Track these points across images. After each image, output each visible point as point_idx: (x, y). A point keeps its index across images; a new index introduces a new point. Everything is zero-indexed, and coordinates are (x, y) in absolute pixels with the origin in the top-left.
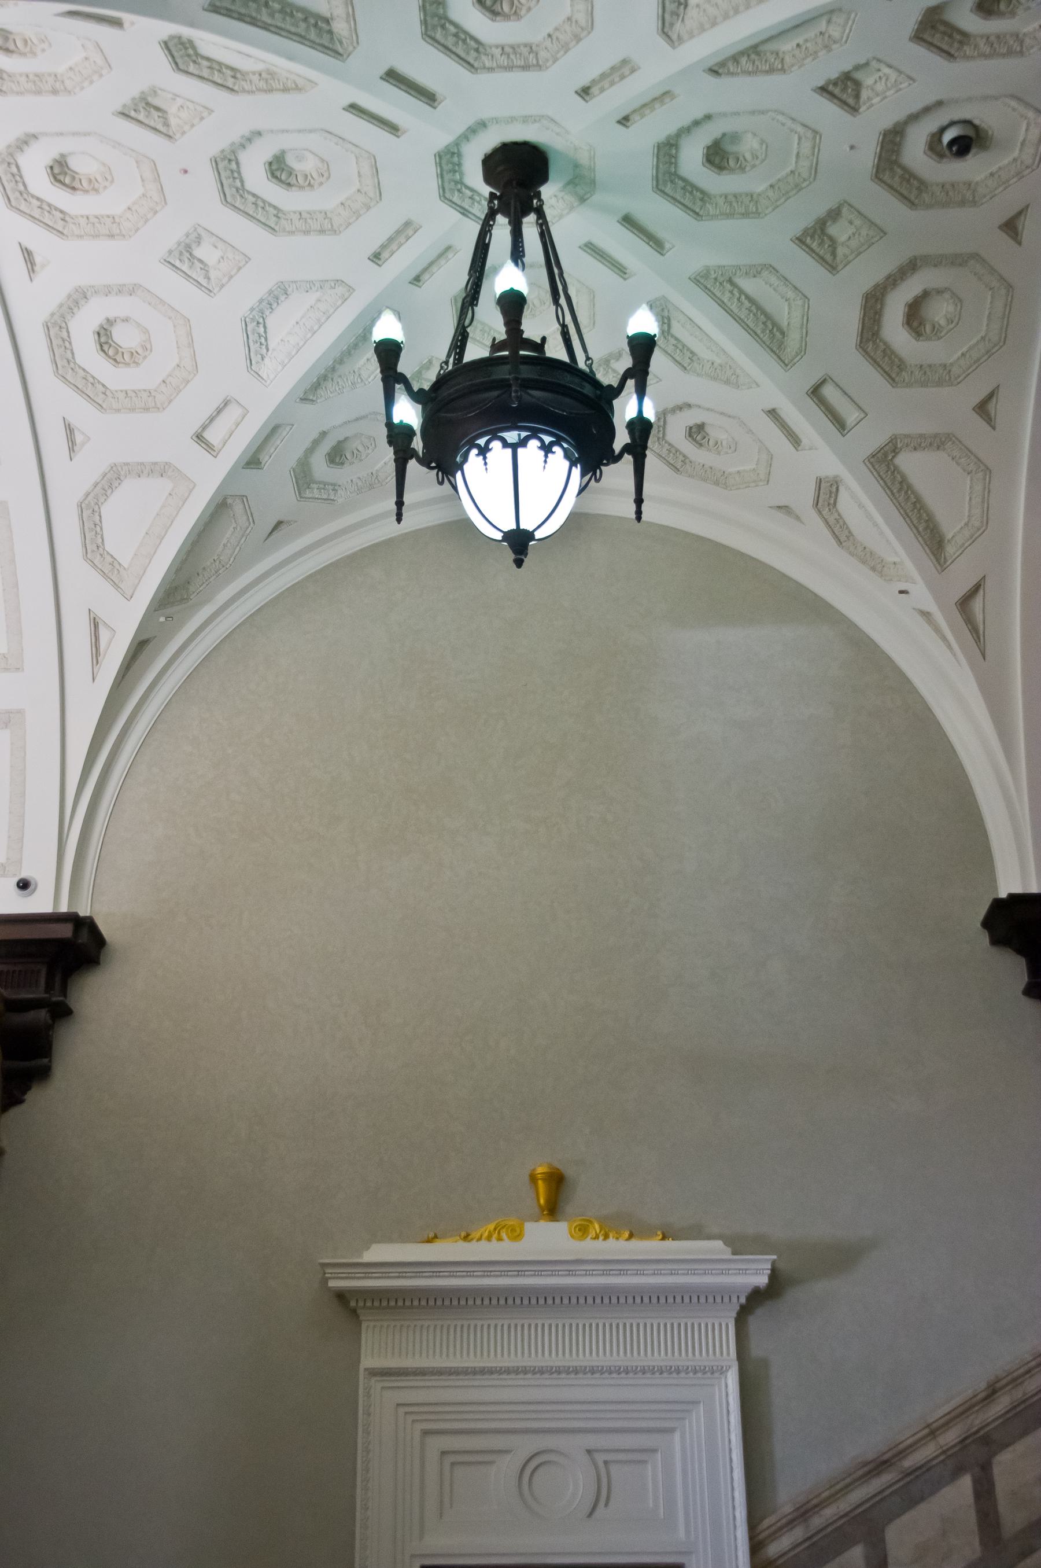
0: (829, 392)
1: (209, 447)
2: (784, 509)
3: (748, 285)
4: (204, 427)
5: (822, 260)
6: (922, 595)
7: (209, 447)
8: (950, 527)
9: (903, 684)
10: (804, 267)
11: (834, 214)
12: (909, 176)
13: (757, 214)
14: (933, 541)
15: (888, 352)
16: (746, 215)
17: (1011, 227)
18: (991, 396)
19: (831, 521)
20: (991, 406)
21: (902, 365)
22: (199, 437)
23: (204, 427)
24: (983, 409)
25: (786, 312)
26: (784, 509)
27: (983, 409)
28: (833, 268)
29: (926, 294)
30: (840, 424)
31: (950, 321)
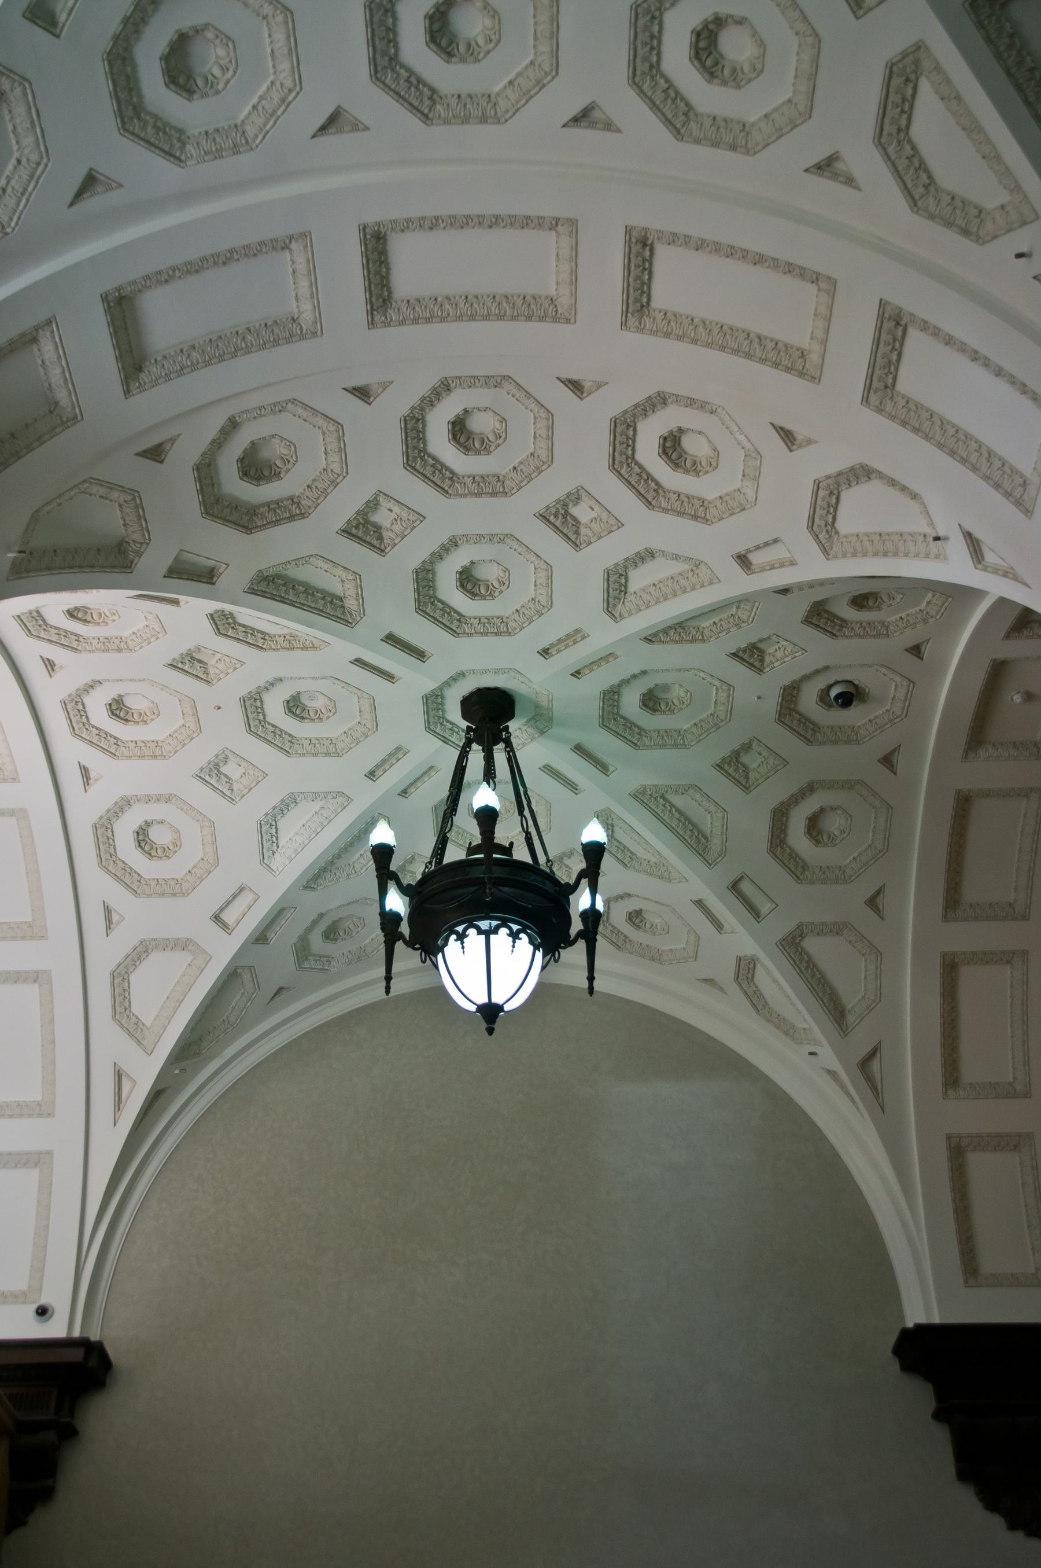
0: (746, 887)
1: (224, 926)
2: (710, 982)
3: (678, 800)
4: (222, 909)
5: (737, 782)
6: (828, 1057)
7: (224, 926)
8: (850, 999)
9: (816, 1134)
10: (724, 789)
11: (747, 747)
12: (804, 720)
13: (684, 746)
14: (836, 1012)
15: (794, 856)
16: (675, 746)
17: (888, 761)
18: (878, 892)
19: (750, 992)
20: (879, 901)
21: (805, 867)
22: (217, 918)
23: (222, 909)
24: (872, 902)
25: (709, 823)
26: (710, 982)
27: (872, 902)
28: (746, 789)
29: (822, 810)
30: (755, 913)
31: (842, 832)
